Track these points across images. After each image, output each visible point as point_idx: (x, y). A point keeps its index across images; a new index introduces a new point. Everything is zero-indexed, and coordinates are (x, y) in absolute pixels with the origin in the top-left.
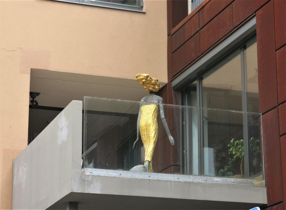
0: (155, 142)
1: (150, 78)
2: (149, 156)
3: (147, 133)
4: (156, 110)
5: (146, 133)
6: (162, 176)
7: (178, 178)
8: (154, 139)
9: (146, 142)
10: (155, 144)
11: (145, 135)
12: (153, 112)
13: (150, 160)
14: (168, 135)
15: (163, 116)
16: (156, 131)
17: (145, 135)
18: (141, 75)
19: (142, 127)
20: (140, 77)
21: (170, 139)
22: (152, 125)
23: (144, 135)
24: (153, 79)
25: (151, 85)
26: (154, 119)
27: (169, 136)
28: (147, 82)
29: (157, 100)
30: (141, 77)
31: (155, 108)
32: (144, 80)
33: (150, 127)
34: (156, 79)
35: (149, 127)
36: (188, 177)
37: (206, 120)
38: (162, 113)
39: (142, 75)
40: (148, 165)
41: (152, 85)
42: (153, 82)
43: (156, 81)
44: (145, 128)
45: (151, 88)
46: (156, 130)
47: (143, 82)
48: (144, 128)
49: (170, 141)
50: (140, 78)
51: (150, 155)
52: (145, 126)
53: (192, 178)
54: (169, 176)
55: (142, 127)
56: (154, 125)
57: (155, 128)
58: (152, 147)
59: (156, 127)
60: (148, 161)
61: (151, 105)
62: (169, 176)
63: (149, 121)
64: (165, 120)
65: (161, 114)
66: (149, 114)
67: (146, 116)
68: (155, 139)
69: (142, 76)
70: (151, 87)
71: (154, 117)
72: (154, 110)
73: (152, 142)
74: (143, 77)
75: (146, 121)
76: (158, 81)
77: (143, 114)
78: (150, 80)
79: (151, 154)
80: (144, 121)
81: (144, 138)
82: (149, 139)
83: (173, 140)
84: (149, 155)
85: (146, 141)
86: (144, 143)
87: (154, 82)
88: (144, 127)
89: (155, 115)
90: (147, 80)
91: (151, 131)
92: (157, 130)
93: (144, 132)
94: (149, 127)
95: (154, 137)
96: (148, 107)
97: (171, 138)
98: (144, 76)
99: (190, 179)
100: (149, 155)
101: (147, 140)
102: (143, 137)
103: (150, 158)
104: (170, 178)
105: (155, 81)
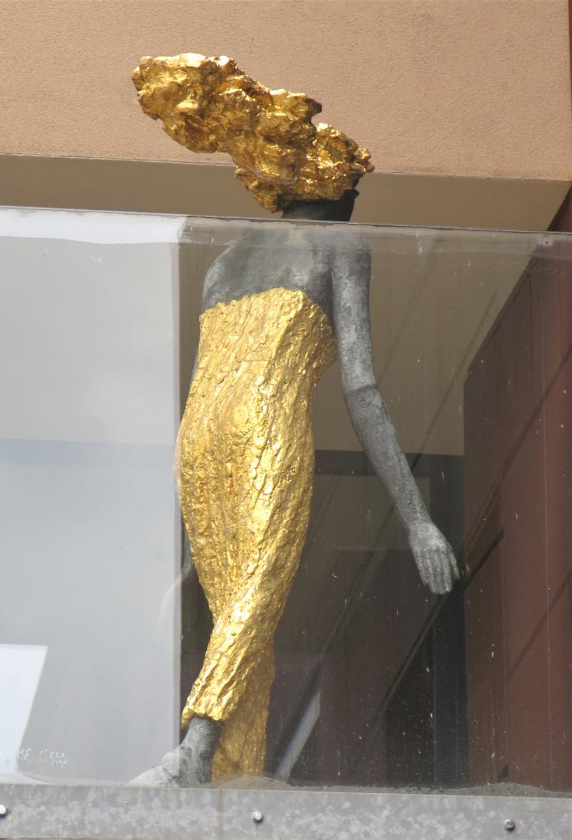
0: (274, 570)
1: (249, 88)
2: (214, 682)
3: (220, 507)
4: (302, 330)
5: (214, 505)
6: (112, 810)
7: (259, 822)
8: (270, 551)
9: (220, 575)
10: (273, 585)
11: (209, 527)
12: (274, 345)
13: (217, 714)
14: (403, 511)
15: (358, 374)
16: (290, 489)
17: (209, 527)
18: (164, 67)
19: (192, 468)
20: (159, 80)
21: (417, 549)
22: (260, 442)
23: (204, 523)
24: (273, 93)
25: (261, 141)
26: (279, 394)
27: (412, 528)
28: (225, 121)
29: (315, 252)
30: (167, 79)
31: (292, 314)
32: (187, 105)
33: (239, 459)
34: (303, 94)
35: (235, 461)
36: (347, 805)
37: (302, 288)
38: (351, 350)
39: (171, 61)
40: (202, 748)
41: (269, 139)
42: (278, 114)
43: (303, 110)
44: (212, 472)
45: (265, 168)
46: (286, 482)
47: (184, 115)
48: (201, 473)
49: (420, 565)
50: (153, 86)
51: (227, 672)
52: (212, 453)
53: (386, 813)
54: (173, 804)
55: (192, 468)
56: (270, 441)
57: (277, 465)
58: (248, 607)
59: (293, 458)
60: (206, 718)
61: (262, 295)
62: (179, 807)
63: (237, 418)
64: (377, 400)
65: (345, 359)
66: (244, 365)
67: (220, 376)
68: (278, 548)
69: (172, 71)
70: (266, 159)
71: (283, 382)
72: (288, 330)
73: (250, 570)
74: (180, 78)
75: (217, 417)
76: (315, 107)
77: (206, 369)
78: (244, 103)
79: (231, 663)
80: (206, 421)
81: (208, 551)
82: (235, 555)
83: (438, 550)
84: (220, 672)
85: (217, 568)
86: (211, 590)
87: (286, 119)
88: (203, 466)
89: (296, 366)
90: (221, 106)
91: (247, 486)
92: (295, 480)
93: (207, 502)
94: (235, 461)
95: (270, 531)
96: (244, 308)
97: (423, 542)
98: (186, 70)
99: (365, 821)
100: (220, 672)
101: (226, 565)
102: (202, 541)
103: (223, 692)
104: (184, 823)
105: (292, 111)
